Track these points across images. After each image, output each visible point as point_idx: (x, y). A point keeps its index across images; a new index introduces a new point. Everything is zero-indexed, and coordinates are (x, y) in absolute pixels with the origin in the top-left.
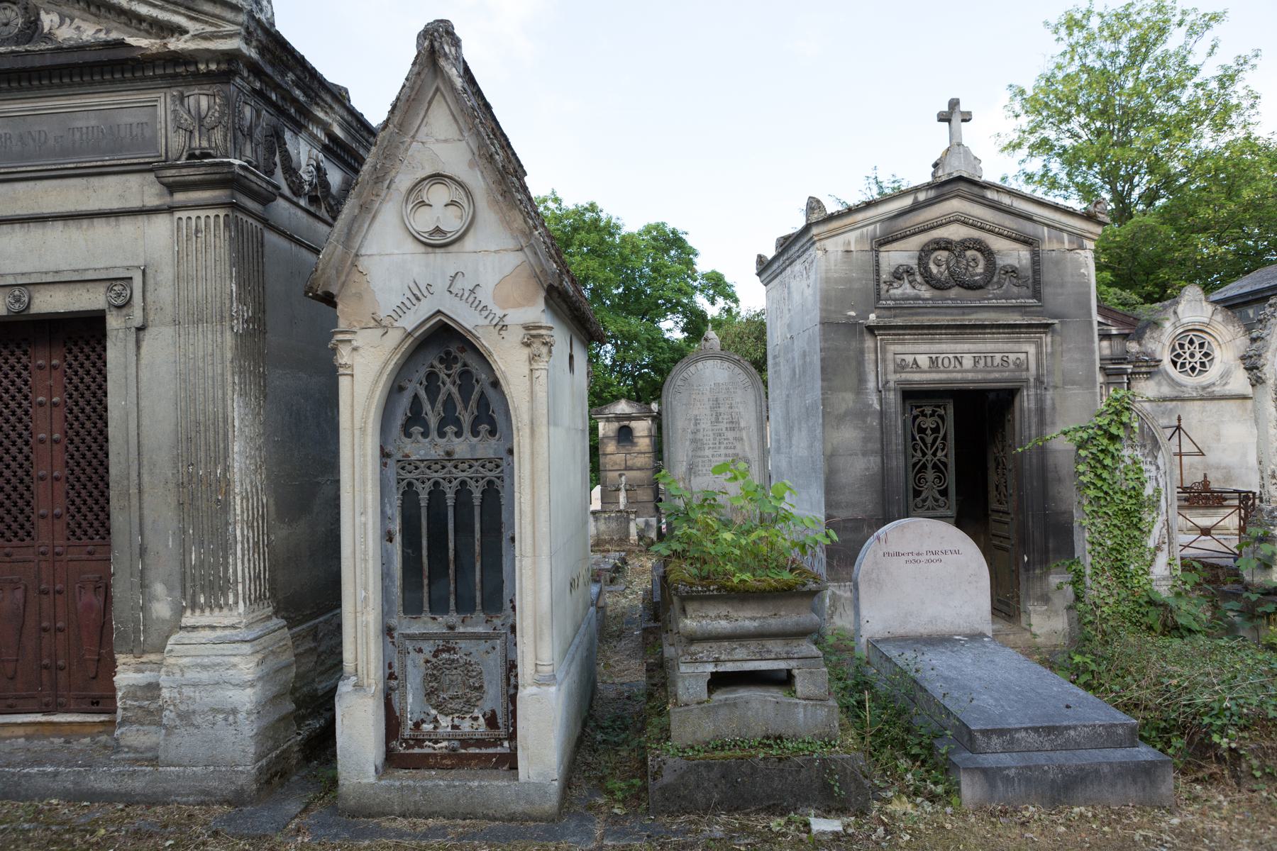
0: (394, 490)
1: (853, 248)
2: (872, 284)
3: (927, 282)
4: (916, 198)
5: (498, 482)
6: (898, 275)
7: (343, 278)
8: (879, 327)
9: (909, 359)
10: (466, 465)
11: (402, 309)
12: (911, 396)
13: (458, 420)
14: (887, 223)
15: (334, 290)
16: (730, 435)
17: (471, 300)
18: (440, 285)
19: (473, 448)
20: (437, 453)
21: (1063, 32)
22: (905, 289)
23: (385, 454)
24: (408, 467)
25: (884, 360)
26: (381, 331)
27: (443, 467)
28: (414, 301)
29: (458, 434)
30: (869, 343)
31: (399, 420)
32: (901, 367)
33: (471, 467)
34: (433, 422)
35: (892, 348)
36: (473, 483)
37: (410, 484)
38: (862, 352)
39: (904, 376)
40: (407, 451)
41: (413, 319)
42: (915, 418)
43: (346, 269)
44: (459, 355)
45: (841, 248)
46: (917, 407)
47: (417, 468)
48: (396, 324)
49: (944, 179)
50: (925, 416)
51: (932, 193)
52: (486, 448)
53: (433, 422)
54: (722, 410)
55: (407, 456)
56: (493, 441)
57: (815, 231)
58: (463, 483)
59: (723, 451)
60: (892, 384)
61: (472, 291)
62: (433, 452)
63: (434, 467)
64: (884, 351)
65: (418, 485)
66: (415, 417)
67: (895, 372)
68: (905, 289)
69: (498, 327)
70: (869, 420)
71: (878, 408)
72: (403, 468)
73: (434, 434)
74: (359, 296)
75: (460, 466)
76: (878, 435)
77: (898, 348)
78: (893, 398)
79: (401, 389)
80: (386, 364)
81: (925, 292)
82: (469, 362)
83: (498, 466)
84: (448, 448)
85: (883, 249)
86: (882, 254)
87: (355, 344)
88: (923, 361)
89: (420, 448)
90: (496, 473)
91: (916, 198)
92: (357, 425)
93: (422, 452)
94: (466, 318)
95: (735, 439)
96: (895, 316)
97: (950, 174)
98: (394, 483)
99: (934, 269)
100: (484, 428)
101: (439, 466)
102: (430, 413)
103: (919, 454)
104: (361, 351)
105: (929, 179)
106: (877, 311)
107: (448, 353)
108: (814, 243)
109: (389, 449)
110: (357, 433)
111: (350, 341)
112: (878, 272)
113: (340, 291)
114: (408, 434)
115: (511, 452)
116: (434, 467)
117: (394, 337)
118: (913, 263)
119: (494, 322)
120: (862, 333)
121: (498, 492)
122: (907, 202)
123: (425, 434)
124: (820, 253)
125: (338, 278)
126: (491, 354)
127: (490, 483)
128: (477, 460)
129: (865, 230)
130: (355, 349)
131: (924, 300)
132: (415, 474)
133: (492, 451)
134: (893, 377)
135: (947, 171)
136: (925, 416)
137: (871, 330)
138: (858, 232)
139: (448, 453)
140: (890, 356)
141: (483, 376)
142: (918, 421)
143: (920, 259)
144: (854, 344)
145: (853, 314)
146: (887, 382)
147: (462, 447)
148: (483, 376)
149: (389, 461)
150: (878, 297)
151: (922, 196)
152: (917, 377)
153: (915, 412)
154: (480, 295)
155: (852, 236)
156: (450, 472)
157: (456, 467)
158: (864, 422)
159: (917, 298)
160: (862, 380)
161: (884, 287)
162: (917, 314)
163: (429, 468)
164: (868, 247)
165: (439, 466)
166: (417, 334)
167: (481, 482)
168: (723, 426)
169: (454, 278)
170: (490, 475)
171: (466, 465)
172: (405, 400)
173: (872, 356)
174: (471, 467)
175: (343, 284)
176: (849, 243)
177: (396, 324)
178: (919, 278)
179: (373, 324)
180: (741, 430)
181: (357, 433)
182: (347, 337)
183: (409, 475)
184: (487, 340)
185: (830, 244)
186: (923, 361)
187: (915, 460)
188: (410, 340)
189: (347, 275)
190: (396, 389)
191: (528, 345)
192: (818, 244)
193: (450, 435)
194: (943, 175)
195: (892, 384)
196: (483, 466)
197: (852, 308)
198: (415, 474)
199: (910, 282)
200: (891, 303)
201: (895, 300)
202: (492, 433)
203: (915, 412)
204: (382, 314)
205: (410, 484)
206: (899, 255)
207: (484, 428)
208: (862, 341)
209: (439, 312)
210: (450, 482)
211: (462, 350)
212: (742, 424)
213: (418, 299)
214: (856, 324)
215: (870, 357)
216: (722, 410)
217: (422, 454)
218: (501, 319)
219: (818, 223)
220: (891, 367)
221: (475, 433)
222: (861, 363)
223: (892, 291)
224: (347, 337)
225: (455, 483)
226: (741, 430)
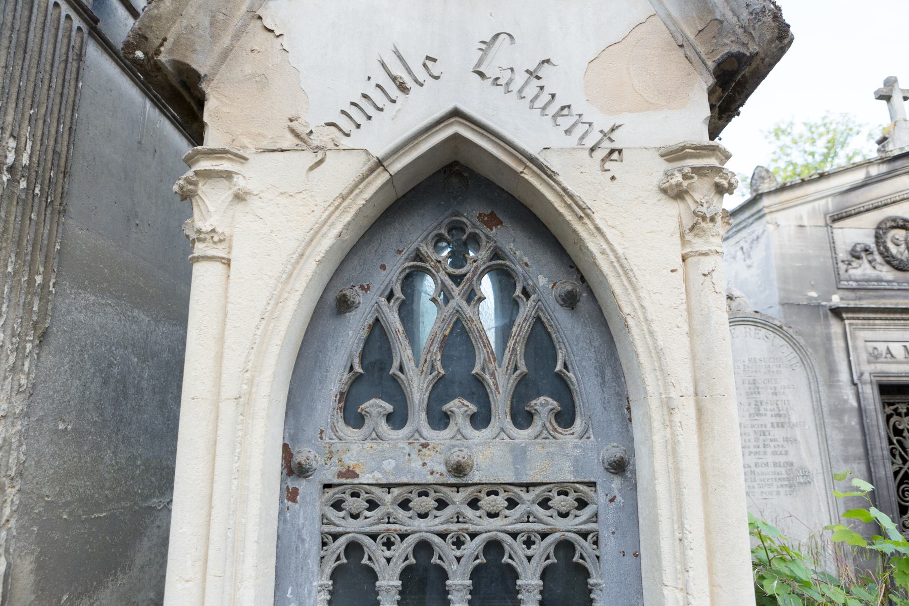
0: (313, 563)
1: (805, 223)
2: (830, 263)
3: (888, 263)
4: (868, 173)
5: (584, 546)
6: (855, 255)
7: (226, 41)
8: (848, 310)
9: (882, 347)
10: (500, 501)
11: (363, 109)
12: (891, 391)
13: (479, 381)
14: (839, 198)
15: (201, 63)
16: (778, 433)
17: (531, 90)
18: (457, 61)
19: (520, 455)
20: (428, 467)
21: (772, 137)
22: (862, 270)
23: (294, 469)
24: (352, 504)
25: (855, 348)
26: (310, 158)
27: (442, 504)
28: (394, 92)
29: (480, 420)
30: (835, 327)
31: (335, 380)
32: (874, 357)
33: (512, 503)
34: (418, 389)
35: (863, 335)
36: (517, 547)
37: (354, 549)
38: (828, 338)
39: (880, 367)
40: (350, 461)
41: (396, 129)
42: (889, 417)
43: (236, 23)
44: (483, 231)
45: (794, 223)
46: (890, 404)
47: (373, 505)
48: (345, 142)
49: (897, 153)
50: (899, 414)
51: (884, 168)
52: (555, 455)
53: (418, 389)
54: (762, 397)
55: (350, 473)
56: (569, 439)
57: (766, 202)
58: (494, 547)
59: (770, 459)
60: (866, 377)
61: (533, 74)
62: (416, 464)
63: (418, 503)
64: (854, 338)
66: (375, 372)
67: (869, 362)
68: (862, 270)
69: (600, 154)
70: (846, 418)
71: (855, 404)
72: (337, 505)
73: (419, 418)
74: (262, 81)
75: (487, 502)
76: (858, 436)
77: (869, 335)
78: (870, 394)
79: (344, 305)
80: (316, 233)
81: (887, 273)
82: (508, 247)
83: (582, 504)
84: (456, 457)
85: (836, 225)
86: (835, 231)
87: (239, 182)
88: (898, 350)
89: (385, 455)
90: (579, 520)
91: (868, 173)
92: (230, 389)
93: (389, 465)
94: (522, 127)
95: (786, 440)
96: (860, 299)
97: (901, 149)
98: (312, 545)
99: (893, 250)
100: (545, 405)
101: (429, 502)
102: (410, 366)
103: (899, 461)
104: (254, 203)
105: (874, 155)
106: (841, 292)
107: (456, 227)
108: (764, 215)
109: (305, 454)
110: (228, 409)
111: (228, 175)
112: (833, 249)
113: (216, 68)
114: (356, 420)
115: (620, 467)
116: (418, 503)
117: (342, 170)
118: (871, 242)
119: (589, 142)
120: (826, 317)
121: (586, 574)
122: (859, 176)
123: (397, 419)
124: (771, 227)
125: (215, 38)
126: (584, 213)
127: (565, 547)
128: (528, 486)
129: (816, 204)
130: (239, 197)
131: (887, 282)
132: (370, 522)
133: (567, 465)
134: (868, 369)
135: (898, 146)
136: (899, 414)
137: (837, 312)
138: (809, 206)
139: (459, 469)
140: (860, 343)
141: (542, 281)
142: (892, 420)
143: (877, 237)
144: (819, 329)
145: (814, 294)
146: (862, 374)
147: (493, 452)
148: (542, 281)
149: (303, 485)
150: (838, 278)
151: (874, 171)
152: (893, 368)
153: (889, 410)
154: (551, 79)
155: (804, 210)
156: (459, 518)
157: (474, 504)
158: (841, 421)
159: (879, 280)
160: (832, 371)
161: (843, 267)
162: (883, 297)
163: (404, 505)
164: (822, 223)
165: (429, 502)
166: (397, 166)
167: (540, 548)
168: (768, 420)
169: (488, 45)
170: (565, 527)
171: (500, 501)
172: (351, 334)
173: (842, 344)
174: (512, 503)
175: (225, 56)
176: (801, 218)
177: (345, 142)
178: (879, 258)
179: (289, 141)
180: (792, 426)
181: (228, 409)
182: (225, 165)
183: (352, 525)
184: (574, 177)
185: (780, 217)
186: (898, 350)
187: (896, 467)
188: (381, 179)
189: (237, 37)
190: (334, 303)
191: (678, 194)
192: (768, 218)
193: (460, 422)
194: (894, 149)
195: (866, 377)
196: (544, 503)
197: (813, 288)
198: (370, 522)
199: (870, 262)
200: (854, 284)
201: (856, 281)
202: (565, 417)
203: (889, 410)
204: (313, 120)
205: (354, 549)
206: (857, 232)
207: (545, 405)
208: (828, 326)
209: (456, 113)
210: (459, 543)
211: (492, 221)
212: (794, 419)
213: (403, 88)
214: (819, 306)
215: (838, 344)
216: (762, 397)
217: (387, 471)
218: (607, 135)
219: (769, 193)
220: (864, 357)
221: (522, 417)
222: (829, 351)
223: (851, 272)
224: (225, 165)
225: (472, 547)
226: (792, 426)
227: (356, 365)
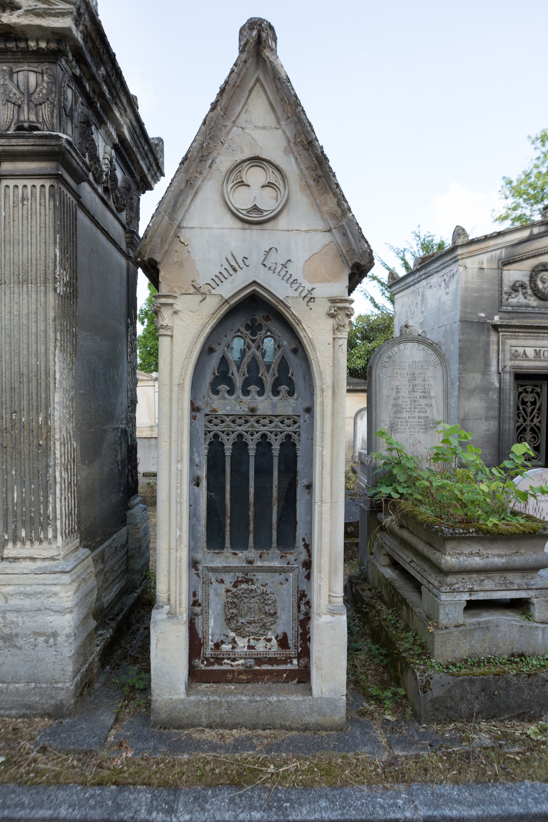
0: (202, 440)
1: (485, 266)
2: (497, 294)
3: (535, 295)
4: (531, 232)
5: (295, 436)
6: (515, 288)
7: (166, 247)
8: (502, 326)
9: (521, 350)
10: (267, 421)
11: (220, 278)
12: (522, 378)
13: (261, 380)
14: (510, 249)
16: (423, 402)
17: (283, 273)
18: (255, 259)
19: (274, 405)
20: (242, 409)
21: (539, 143)
22: (518, 299)
23: (195, 409)
24: (215, 421)
25: (503, 351)
26: (200, 297)
27: (247, 422)
28: (231, 272)
29: (261, 393)
30: (493, 337)
31: (209, 378)
32: (515, 356)
33: (271, 422)
34: (239, 381)
35: (510, 342)
36: (272, 436)
37: (216, 436)
38: (488, 344)
39: (517, 363)
40: (214, 406)
41: (231, 288)
42: (520, 394)
43: (169, 239)
44: (264, 323)
45: (477, 266)
46: (522, 386)
47: (222, 422)
48: (213, 292)
52: (286, 406)
53: (239, 381)
54: (417, 382)
55: (215, 411)
56: (292, 400)
57: (460, 251)
59: (417, 414)
60: (508, 369)
61: (284, 266)
62: (238, 408)
63: (238, 421)
64: (504, 344)
65: (272, 438)
66: (223, 377)
67: (511, 360)
68: (518, 299)
69: (307, 299)
70: (491, 394)
71: (498, 385)
72: (210, 422)
73: (239, 392)
74: (180, 264)
75: (262, 421)
76: (496, 405)
77: (513, 342)
78: (508, 378)
79: (211, 351)
80: (204, 327)
81: (533, 302)
83: (295, 422)
84: (252, 406)
85: (505, 268)
86: (505, 272)
87: (176, 307)
88: (530, 352)
89: (227, 405)
90: (294, 428)
91: (531, 232)
92: (176, 381)
93: (228, 408)
94: (278, 289)
95: (426, 405)
96: (512, 319)
98: (202, 434)
99: (540, 285)
100: (284, 388)
101: (242, 421)
102: (236, 373)
103: (521, 420)
104: (181, 314)
106: (500, 314)
107: (253, 321)
109: (199, 403)
110: (175, 388)
111: (172, 305)
112: (501, 285)
114: (216, 392)
115: (309, 410)
116: (238, 421)
118: (526, 280)
119: (303, 295)
120: (488, 330)
121: (295, 445)
122: (525, 234)
123: (231, 392)
124: (461, 269)
125: (162, 246)
126: (299, 322)
127: (288, 436)
128: (276, 416)
129: (494, 253)
130: (175, 313)
131: (533, 307)
132: (221, 427)
134: (509, 363)
136: (527, 392)
137: (496, 328)
138: (490, 254)
139: (253, 410)
140: (507, 348)
141: (285, 343)
143: (531, 277)
144: (483, 338)
145: (483, 315)
146: (505, 367)
147: (264, 404)
148: (285, 343)
149: (198, 415)
151: (536, 230)
152: (525, 364)
153: (521, 389)
154: (291, 268)
155: (485, 257)
156: (252, 426)
157: (258, 422)
158: (488, 395)
159: (527, 306)
160: (487, 364)
161: (505, 296)
163: (234, 422)
164: (495, 266)
165: (242, 421)
166: (233, 302)
167: (280, 436)
168: (418, 394)
169: (268, 252)
170: (289, 430)
171: (267, 421)
172: (214, 361)
173: (495, 347)
174: (271, 422)
175: (166, 252)
176: (482, 263)
177: (213, 292)
178: (529, 291)
179: (192, 290)
180: (431, 398)
181: (175, 388)
182: (170, 301)
183: (215, 428)
184: (297, 310)
185: (469, 262)
186: (530, 352)
187: (518, 424)
189: (170, 245)
190: (207, 350)
191: (333, 316)
192: (460, 262)
193: (254, 394)
195: (508, 369)
196: (282, 422)
197: (483, 311)
198: (221, 427)
199: (523, 294)
200: (510, 309)
201: (512, 306)
202: (291, 393)
203: (521, 389)
204: (201, 282)
205: (216, 436)
206: (517, 273)
207: (284, 388)
208: (489, 336)
209: (255, 282)
210: (252, 435)
211: (267, 319)
212: (432, 394)
213: (235, 270)
214: (485, 323)
215: (493, 348)
216: (417, 382)
217: (228, 409)
218: (310, 292)
219: (462, 246)
220: (508, 356)
221: (276, 393)
222: (487, 352)
223: (510, 300)
224: (170, 301)
225: (257, 436)
226: (431, 398)
227: (215, 373)
